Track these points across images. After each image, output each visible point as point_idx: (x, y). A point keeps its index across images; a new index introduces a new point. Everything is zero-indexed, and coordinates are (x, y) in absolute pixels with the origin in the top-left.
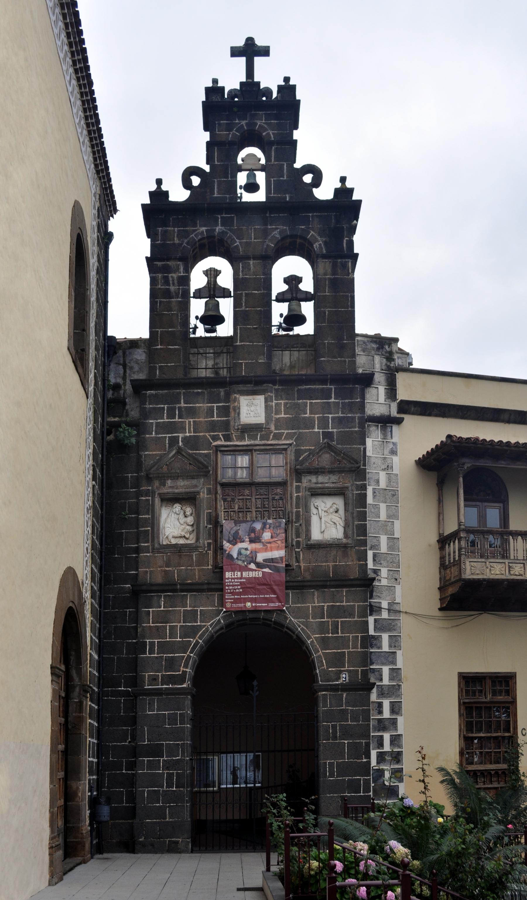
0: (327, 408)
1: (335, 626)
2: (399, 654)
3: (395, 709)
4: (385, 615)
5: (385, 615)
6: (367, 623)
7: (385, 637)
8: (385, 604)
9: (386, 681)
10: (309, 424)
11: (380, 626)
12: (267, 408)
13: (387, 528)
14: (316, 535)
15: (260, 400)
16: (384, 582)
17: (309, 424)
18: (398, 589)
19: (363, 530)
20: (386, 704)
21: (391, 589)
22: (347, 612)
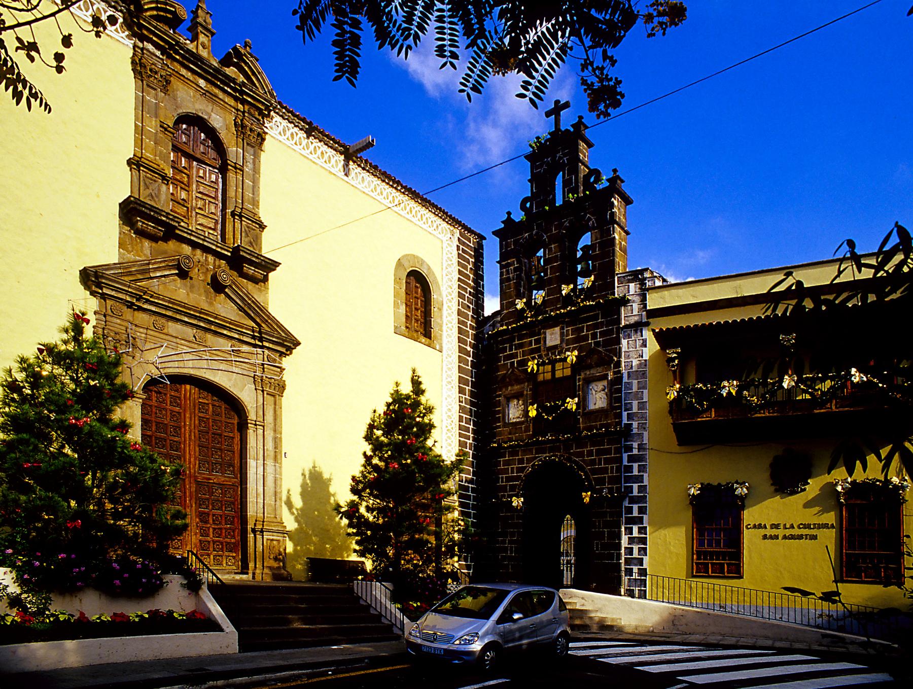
0: (596, 326)
1: (600, 460)
2: (646, 476)
3: (642, 510)
4: (635, 452)
5: (635, 452)
6: (622, 457)
7: (635, 466)
8: (635, 445)
9: (635, 492)
10: (585, 338)
11: (632, 459)
12: (562, 334)
13: (638, 396)
14: (592, 407)
15: (557, 329)
16: (635, 431)
17: (585, 338)
18: (646, 434)
19: (619, 400)
20: (635, 507)
21: (640, 436)
22: (608, 451)
